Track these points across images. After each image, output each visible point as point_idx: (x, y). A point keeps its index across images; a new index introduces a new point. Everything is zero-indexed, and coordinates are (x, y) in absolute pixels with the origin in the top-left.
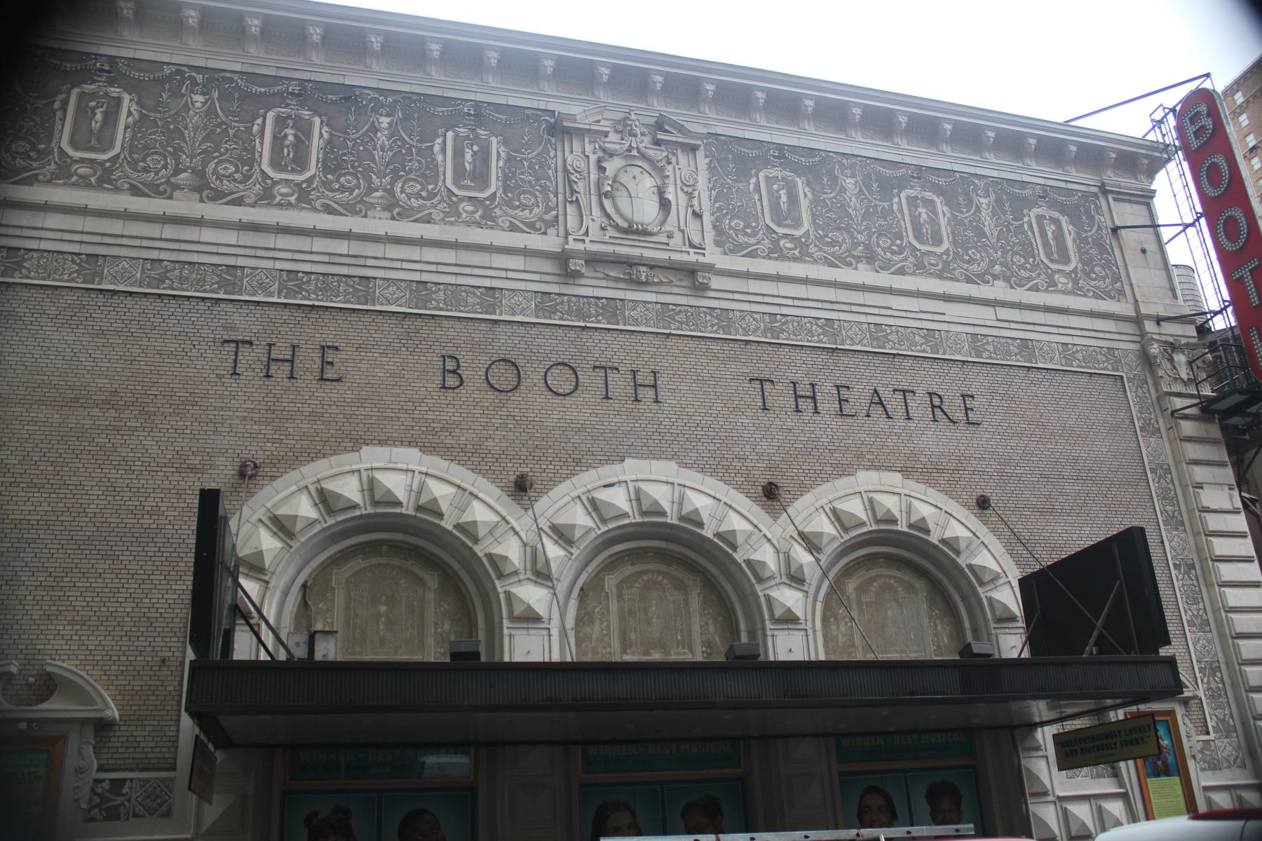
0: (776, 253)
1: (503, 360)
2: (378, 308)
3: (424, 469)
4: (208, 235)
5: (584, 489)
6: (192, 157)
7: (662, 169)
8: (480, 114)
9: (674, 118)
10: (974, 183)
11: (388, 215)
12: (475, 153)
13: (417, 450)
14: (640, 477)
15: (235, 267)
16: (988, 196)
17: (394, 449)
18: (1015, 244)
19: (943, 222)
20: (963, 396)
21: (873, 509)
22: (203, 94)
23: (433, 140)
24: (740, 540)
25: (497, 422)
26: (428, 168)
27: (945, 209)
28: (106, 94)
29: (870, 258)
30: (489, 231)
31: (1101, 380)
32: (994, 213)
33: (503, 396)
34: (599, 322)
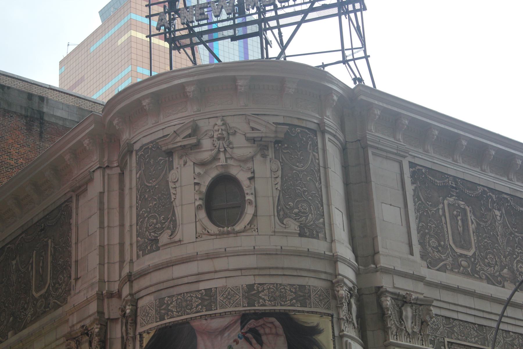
6: (505, 257)
22: (499, 210)
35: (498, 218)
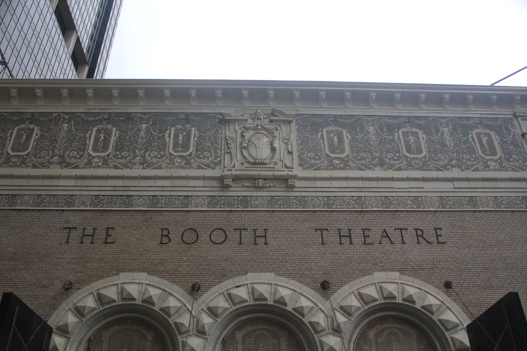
0: (332, 166)
1: (191, 229)
2: (133, 209)
3: (148, 282)
4: (62, 182)
5: (226, 289)
6: (59, 150)
7: (273, 133)
8: (187, 118)
9: (279, 109)
10: (440, 121)
11: (142, 167)
12: (184, 136)
13: (146, 273)
14: (254, 281)
15: (73, 195)
16: (448, 126)
17: (135, 273)
18: (464, 149)
19: (422, 142)
20: (435, 229)
21: (382, 292)
22: (68, 123)
23: (165, 132)
24: (306, 311)
25: (185, 258)
26: (161, 144)
27: (424, 136)
28: (28, 128)
29: (382, 164)
30: (188, 170)
31: (519, 214)
32: (452, 134)
33: (189, 246)
34: (239, 208)
35: (65, 128)
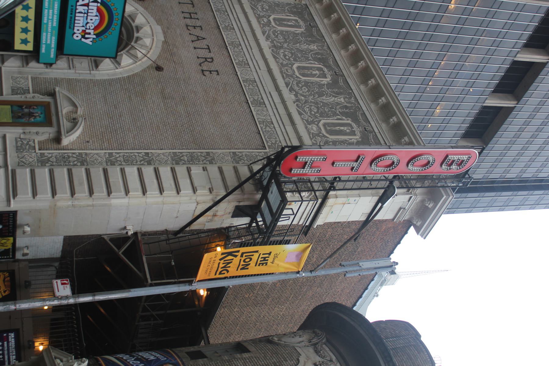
29: (275, 48)
